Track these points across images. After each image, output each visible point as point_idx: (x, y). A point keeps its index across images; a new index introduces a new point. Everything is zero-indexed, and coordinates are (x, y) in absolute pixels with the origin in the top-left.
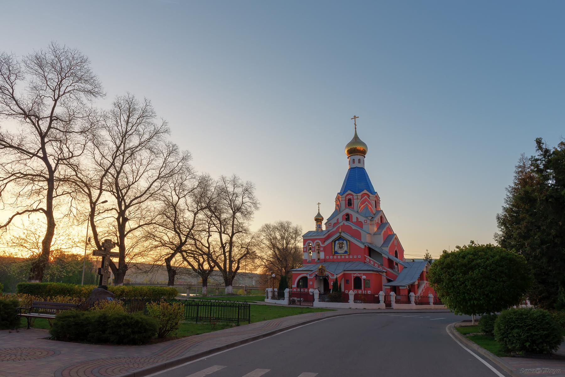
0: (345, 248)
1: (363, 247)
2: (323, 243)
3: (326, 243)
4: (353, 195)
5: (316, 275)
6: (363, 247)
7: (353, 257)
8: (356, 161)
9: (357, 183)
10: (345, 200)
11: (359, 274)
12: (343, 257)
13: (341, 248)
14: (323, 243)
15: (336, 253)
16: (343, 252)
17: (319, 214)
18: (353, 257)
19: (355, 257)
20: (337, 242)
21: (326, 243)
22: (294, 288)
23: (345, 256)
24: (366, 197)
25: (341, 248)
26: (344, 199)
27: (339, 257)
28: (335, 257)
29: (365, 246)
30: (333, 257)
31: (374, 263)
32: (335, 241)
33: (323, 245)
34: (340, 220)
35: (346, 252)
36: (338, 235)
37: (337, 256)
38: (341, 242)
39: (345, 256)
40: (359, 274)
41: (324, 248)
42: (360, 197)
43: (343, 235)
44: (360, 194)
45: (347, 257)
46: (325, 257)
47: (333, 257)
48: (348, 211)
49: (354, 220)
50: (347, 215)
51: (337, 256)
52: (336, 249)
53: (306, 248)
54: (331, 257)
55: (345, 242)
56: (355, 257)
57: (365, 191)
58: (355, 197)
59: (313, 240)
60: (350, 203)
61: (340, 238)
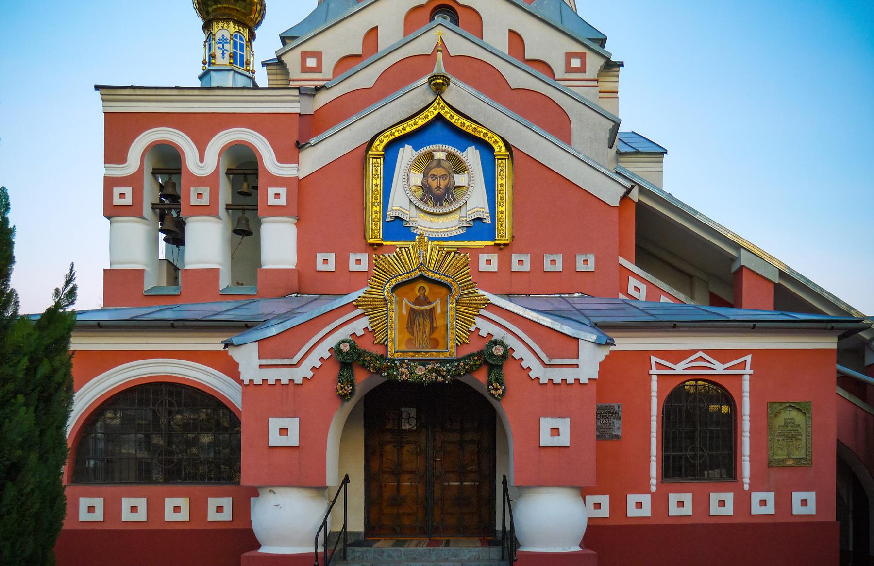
0: (476, 202)
1: (611, 194)
3: (312, 160)
5: (348, 359)
6: (611, 194)
7: (538, 262)
13: (438, 196)
15: (398, 228)
16: (450, 224)
18: (538, 262)
19: (554, 263)
20: (407, 154)
21: (312, 160)
33: (288, 171)
35: (478, 228)
41: (299, 188)
45: (489, 263)
46: (306, 249)
54: (358, 262)
55: (472, 156)
56: (554, 263)
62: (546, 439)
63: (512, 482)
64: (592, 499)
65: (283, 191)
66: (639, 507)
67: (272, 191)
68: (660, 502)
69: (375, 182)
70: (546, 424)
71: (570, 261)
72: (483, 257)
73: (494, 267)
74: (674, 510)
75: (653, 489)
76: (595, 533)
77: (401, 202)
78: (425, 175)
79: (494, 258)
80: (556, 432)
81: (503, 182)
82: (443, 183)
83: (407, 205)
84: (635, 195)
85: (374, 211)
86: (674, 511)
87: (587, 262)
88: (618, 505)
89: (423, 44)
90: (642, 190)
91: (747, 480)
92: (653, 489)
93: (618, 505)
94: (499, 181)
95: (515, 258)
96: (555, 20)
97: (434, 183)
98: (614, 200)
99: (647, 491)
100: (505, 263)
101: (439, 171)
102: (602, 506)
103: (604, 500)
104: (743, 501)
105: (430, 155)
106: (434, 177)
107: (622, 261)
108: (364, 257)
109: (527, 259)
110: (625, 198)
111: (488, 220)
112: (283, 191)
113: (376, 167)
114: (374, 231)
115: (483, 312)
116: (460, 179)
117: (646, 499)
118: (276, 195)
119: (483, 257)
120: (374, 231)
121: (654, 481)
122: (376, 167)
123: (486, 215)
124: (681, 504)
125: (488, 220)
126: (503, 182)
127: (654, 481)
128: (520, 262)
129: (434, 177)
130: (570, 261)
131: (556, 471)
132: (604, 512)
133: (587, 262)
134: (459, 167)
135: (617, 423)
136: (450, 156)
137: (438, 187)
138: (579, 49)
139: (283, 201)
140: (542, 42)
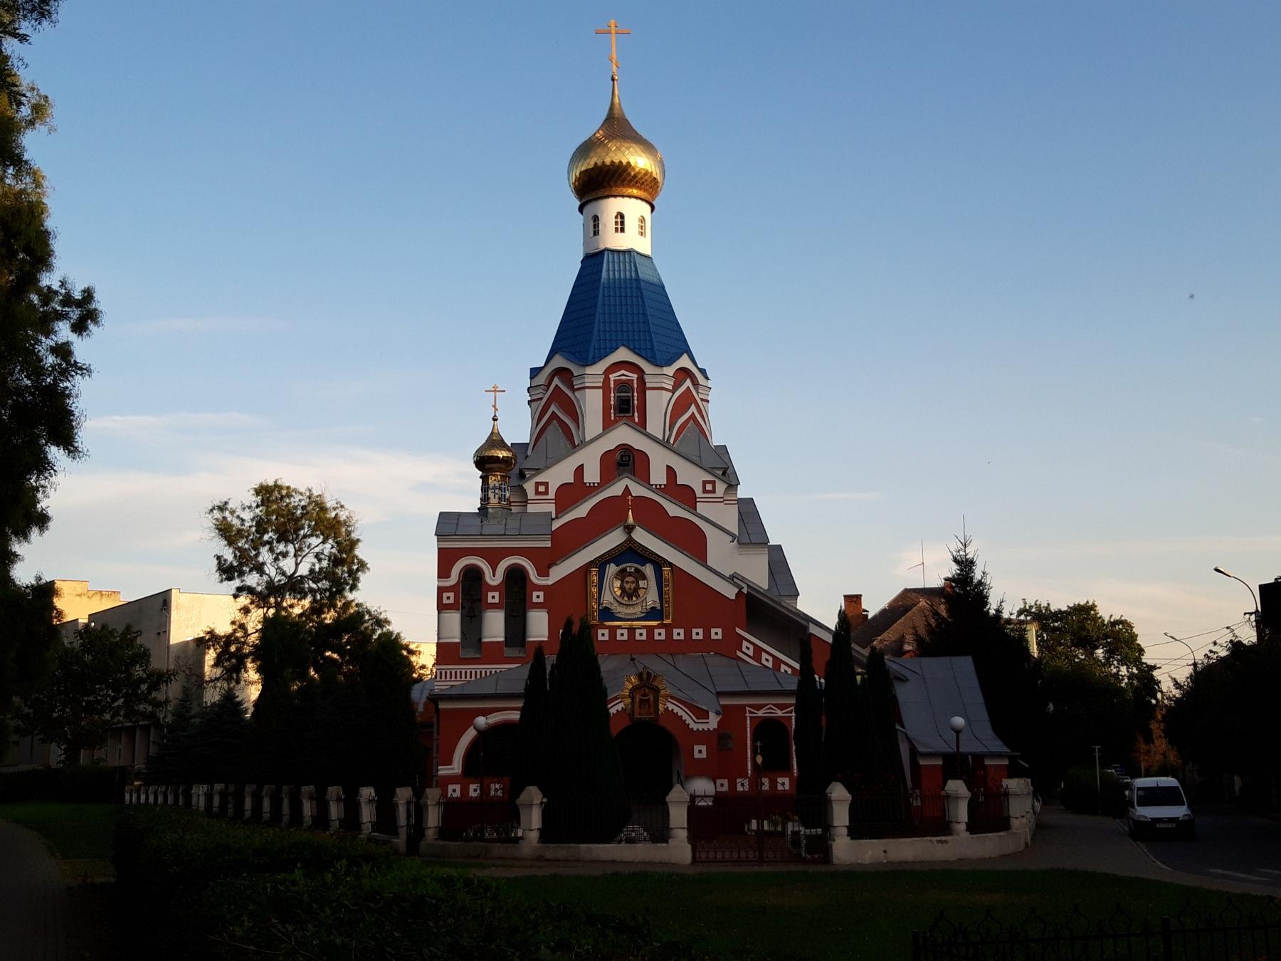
1: (730, 592)
2: (543, 572)
4: (640, 372)
7: (688, 634)
8: (631, 224)
9: (614, 317)
10: (605, 387)
11: (781, 707)
12: (641, 635)
13: (630, 594)
14: (543, 572)
15: (607, 614)
18: (688, 634)
19: (698, 634)
20: (612, 569)
22: (452, 779)
24: (688, 383)
25: (630, 594)
26: (599, 381)
27: (622, 635)
29: (741, 588)
31: (777, 662)
32: (601, 563)
34: (592, 475)
35: (652, 614)
36: (614, 539)
37: (613, 630)
38: (630, 567)
39: (650, 630)
42: (669, 384)
43: (642, 537)
44: (670, 370)
45: (660, 634)
48: (624, 435)
49: (658, 476)
50: (626, 450)
52: (607, 599)
55: (649, 570)
56: (698, 634)
57: (684, 362)
58: (650, 381)
59: (494, 557)
60: (625, 406)
61: (630, 553)
64: (719, 782)
65: (541, 594)
66: (742, 786)
67: (535, 594)
71: (707, 633)
72: (657, 631)
76: (718, 797)
77: (607, 599)
79: (663, 631)
82: (633, 586)
88: (733, 785)
89: (616, 490)
93: (733, 785)
95: (675, 631)
97: (627, 586)
100: (669, 635)
101: (630, 579)
102: (724, 785)
103: (725, 782)
107: (738, 630)
110: (739, 594)
112: (541, 594)
116: (642, 584)
117: (746, 782)
118: (537, 597)
119: (657, 631)
128: (678, 634)
130: (707, 633)
131: (702, 769)
132: (726, 788)
133: (717, 633)
134: (644, 578)
139: (541, 600)
140: (690, 476)
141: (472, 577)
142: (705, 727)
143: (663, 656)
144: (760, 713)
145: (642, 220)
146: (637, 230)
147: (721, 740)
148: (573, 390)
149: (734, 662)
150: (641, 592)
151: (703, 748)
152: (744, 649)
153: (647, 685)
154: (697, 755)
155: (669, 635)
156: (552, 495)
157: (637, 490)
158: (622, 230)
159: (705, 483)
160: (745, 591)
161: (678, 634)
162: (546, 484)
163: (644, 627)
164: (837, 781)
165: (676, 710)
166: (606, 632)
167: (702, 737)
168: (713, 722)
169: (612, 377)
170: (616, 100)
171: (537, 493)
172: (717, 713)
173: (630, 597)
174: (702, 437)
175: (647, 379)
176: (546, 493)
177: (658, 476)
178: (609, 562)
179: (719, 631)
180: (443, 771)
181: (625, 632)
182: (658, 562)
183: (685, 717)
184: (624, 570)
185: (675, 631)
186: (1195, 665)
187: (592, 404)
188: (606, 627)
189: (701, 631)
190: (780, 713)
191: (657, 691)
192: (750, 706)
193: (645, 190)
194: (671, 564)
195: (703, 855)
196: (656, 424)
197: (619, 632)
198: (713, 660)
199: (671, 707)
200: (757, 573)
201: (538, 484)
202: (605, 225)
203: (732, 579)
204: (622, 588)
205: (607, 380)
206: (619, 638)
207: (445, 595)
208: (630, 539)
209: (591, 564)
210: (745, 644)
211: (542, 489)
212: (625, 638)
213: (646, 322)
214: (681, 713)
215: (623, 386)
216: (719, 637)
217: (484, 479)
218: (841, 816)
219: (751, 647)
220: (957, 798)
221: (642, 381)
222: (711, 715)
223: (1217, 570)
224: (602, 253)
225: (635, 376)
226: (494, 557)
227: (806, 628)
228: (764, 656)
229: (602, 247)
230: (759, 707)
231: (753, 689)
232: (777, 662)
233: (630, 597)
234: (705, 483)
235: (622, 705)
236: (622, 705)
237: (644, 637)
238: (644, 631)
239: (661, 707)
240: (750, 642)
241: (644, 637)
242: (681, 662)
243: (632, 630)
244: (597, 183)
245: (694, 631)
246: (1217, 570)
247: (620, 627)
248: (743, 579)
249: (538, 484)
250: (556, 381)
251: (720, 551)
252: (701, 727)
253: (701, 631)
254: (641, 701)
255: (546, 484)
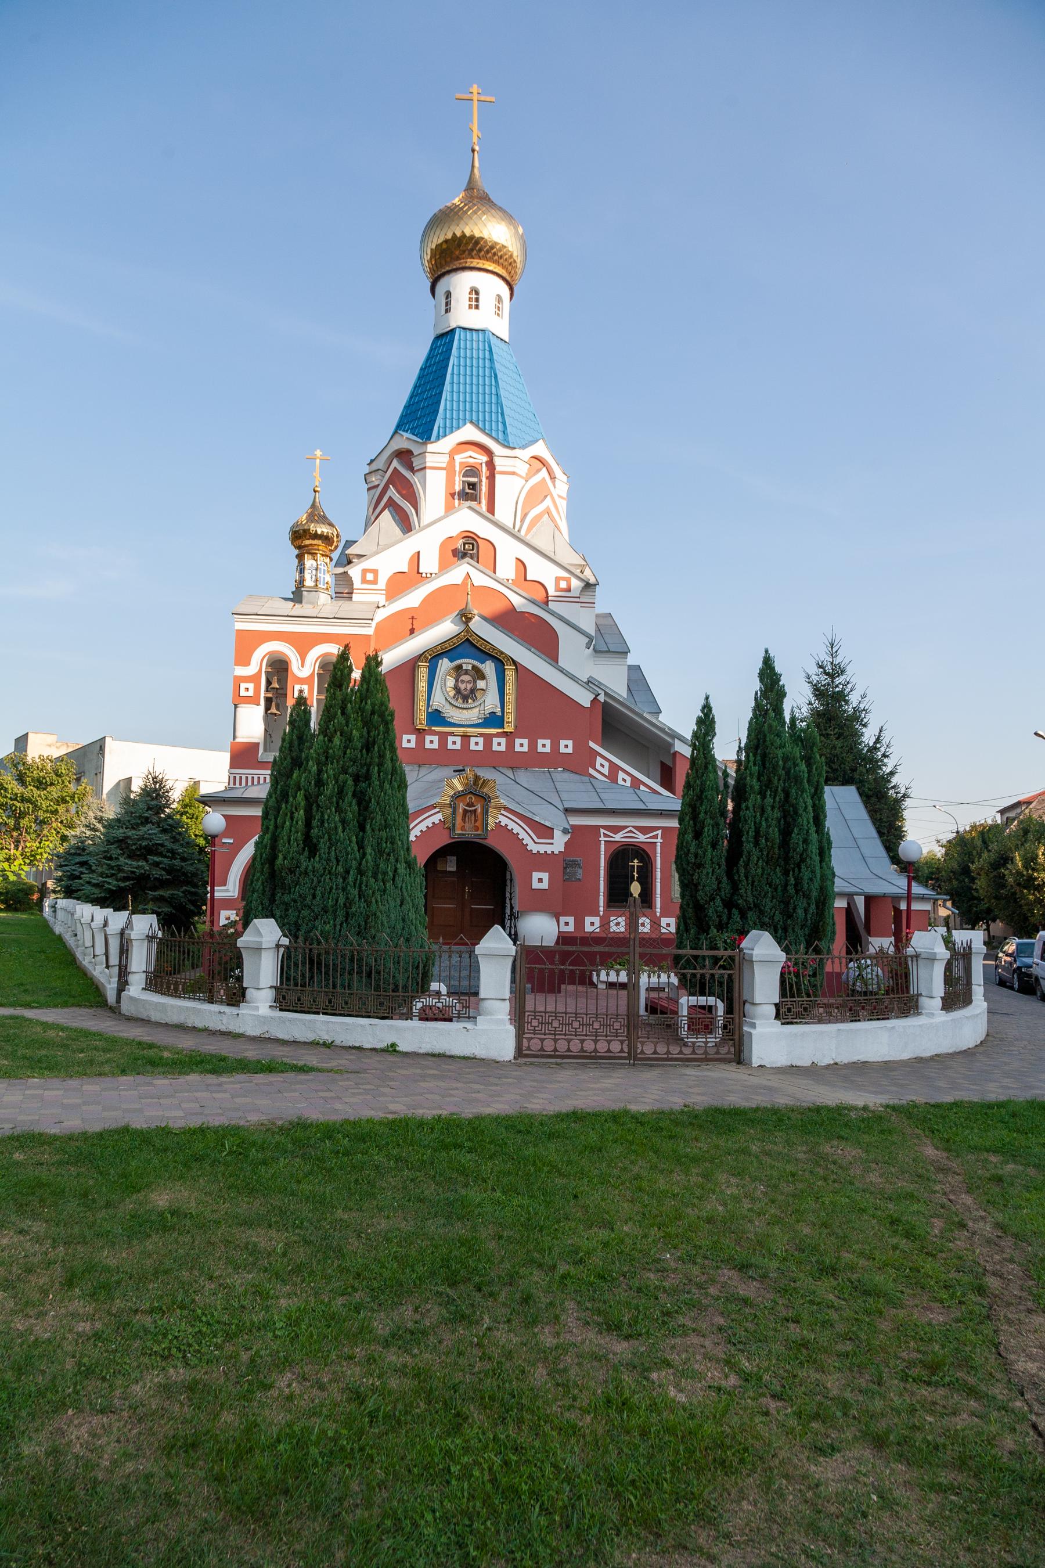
0: (490, 702)
1: (584, 699)
4: (489, 452)
7: (533, 745)
8: (487, 300)
10: (450, 468)
11: (644, 830)
12: (477, 744)
13: (465, 696)
15: (436, 717)
16: (473, 715)
17: (316, 514)
18: (533, 745)
19: (544, 746)
20: (445, 665)
23: (488, 739)
27: (454, 743)
28: (432, 742)
30: (420, 742)
32: (433, 656)
34: (429, 564)
35: (494, 720)
37: (443, 737)
38: (467, 664)
39: (488, 739)
40: (644, 830)
42: (523, 469)
45: (499, 745)
47: (420, 742)
49: (506, 569)
51: (443, 737)
53: (254, 679)
55: (489, 668)
56: (544, 746)
57: (540, 449)
60: (473, 489)
61: (466, 647)
62: (536, 885)
63: (516, 910)
66: (592, 924)
68: (605, 924)
69: (422, 685)
70: (536, 876)
71: (555, 746)
73: (503, 748)
74: (614, 928)
75: (601, 913)
76: (563, 939)
77: (438, 701)
78: (457, 681)
79: (503, 741)
80: (540, 880)
81: (510, 687)
82: (469, 686)
83: (443, 701)
84: (602, 698)
85: (421, 704)
86: (614, 928)
87: (567, 746)
88: (580, 924)
90: (606, 694)
91: (658, 910)
92: (601, 913)
93: (580, 924)
94: (507, 688)
95: (518, 741)
96: (548, 549)
97: (462, 686)
98: (587, 704)
99: (597, 915)
100: (510, 745)
102: (568, 923)
103: (571, 920)
104: (656, 924)
105: (459, 667)
106: (463, 682)
107: (592, 744)
108: (413, 738)
109: (525, 742)
110: (595, 701)
111: (499, 714)
113: (423, 672)
114: (421, 716)
115: (503, 812)
116: (481, 684)
117: (597, 920)
119: (495, 740)
120: (421, 716)
121: (601, 909)
122: (423, 672)
123: (498, 710)
124: (618, 925)
125: (499, 714)
126: (510, 687)
127: (601, 909)
128: (522, 745)
129: (463, 682)
130: (555, 746)
131: (542, 903)
132: (571, 928)
133: (567, 746)
134: (482, 676)
135: (580, 871)
136: (474, 667)
137: (465, 689)
138: (566, 575)
141: (279, 667)
142: (549, 849)
143: (500, 769)
144: (618, 837)
145: (499, 299)
146: (494, 310)
147: (564, 867)
148: (411, 468)
149: (586, 779)
150: (478, 694)
151: (545, 876)
152: (598, 766)
153: (477, 795)
154: (536, 885)
155: (510, 745)
156: (382, 583)
157: (480, 579)
158: (477, 307)
159: (558, 579)
160: (602, 698)
161: (522, 745)
162: (375, 572)
163: (481, 735)
164: (763, 927)
165: (511, 825)
166: (436, 739)
167: (542, 861)
168: (558, 843)
169: (459, 458)
170: (476, 171)
171: (364, 581)
172: (565, 831)
173: (465, 699)
174: (557, 531)
175: (497, 461)
176: (375, 582)
177: (506, 569)
178: (440, 655)
179: (570, 743)
180: (220, 893)
181: (458, 740)
182: (500, 660)
183: (522, 835)
184: (459, 667)
185: (518, 741)
186: (958, 832)
187: (434, 487)
188: (435, 733)
189: (548, 742)
190: (642, 838)
191: (486, 799)
192: (605, 827)
193: (504, 267)
194: (515, 663)
195: (535, 1045)
196: (504, 512)
197: (451, 739)
198: (560, 775)
199: (504, 821)
200: (614, 680)
201: (365, 572)
202: (457, 301)
203: (590, 683)
204: (456, 688)
205: (452, 460)
206: (450, 746)
207: (243, 686)
208: (468, 630)
209: (419, 657)
210: (599, 760)
211: (370, 577)
212: (458, 746)
213: (499, 403)
214: (517, 829)
215: (472, 471)
216: (570, 750)
217: (300, 557)
218: (764, 987)
219: (606, 764)
220: (932, 959)
221: (491, 465)
222: (557, 833)
223: (1036, 734)
224: (453, 331)
225: (484, 459)
226: (303, 643)
227: (671, 745)
228: (621, 775)
229: (453, 325)
230: (616, 829)
231: (610, 805)
232: (636, 783)
233: (465, 699)
234: (558, 579)
235: (440, 816)
236: (440, 816)
237: (480, 747)
238: (481, 740)
239: (491, 820)
240: (605, 758)
241: (480, 747)
242: (522, 776)
243: (466, 738)
244: (452, 255)
245: (540, 742)
246: (1036, 734)
247: (452, 734)
248: (599, 685)
249: (365, 572)
250: (395, 463)
251: (572, 649)
252: (543, 848)
253: (548, 742)
254: (465, 811)
255: (375, 572)
